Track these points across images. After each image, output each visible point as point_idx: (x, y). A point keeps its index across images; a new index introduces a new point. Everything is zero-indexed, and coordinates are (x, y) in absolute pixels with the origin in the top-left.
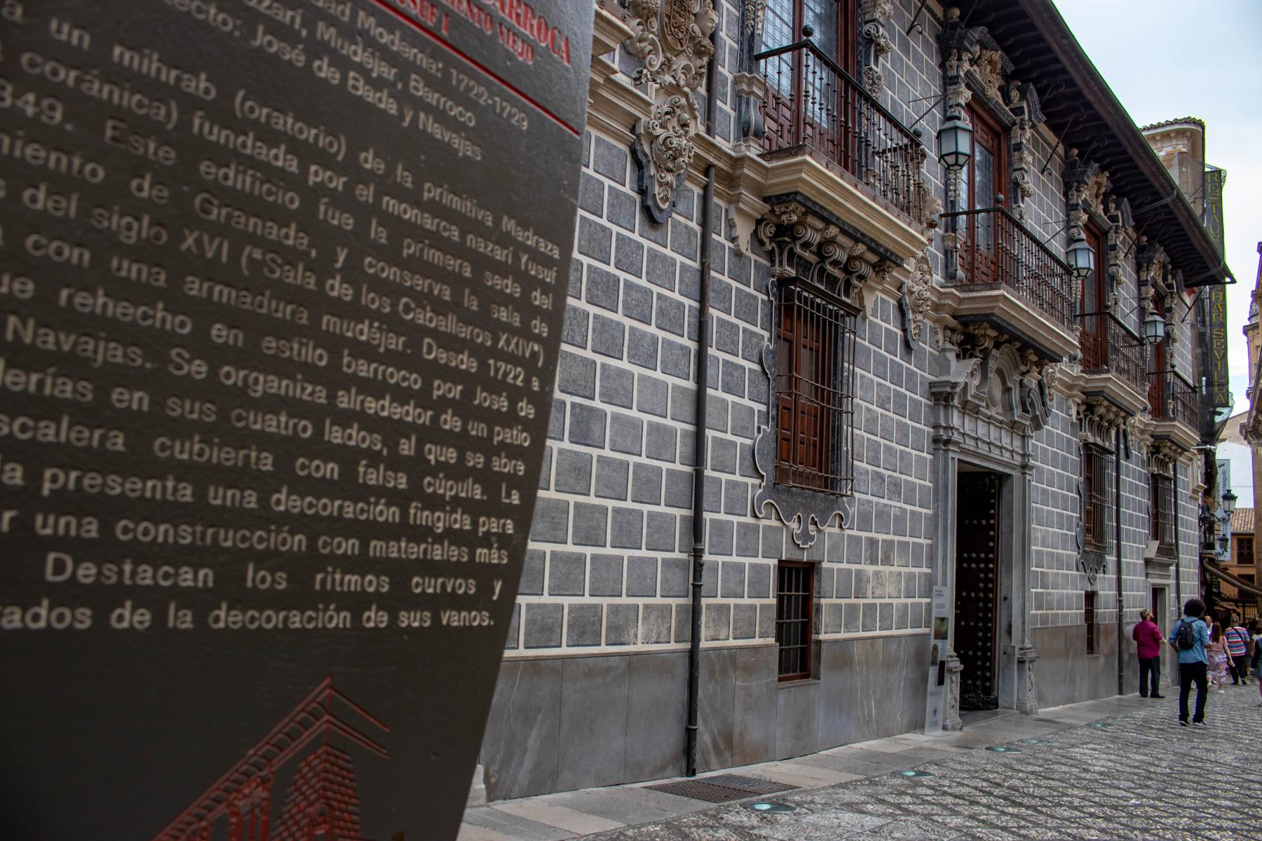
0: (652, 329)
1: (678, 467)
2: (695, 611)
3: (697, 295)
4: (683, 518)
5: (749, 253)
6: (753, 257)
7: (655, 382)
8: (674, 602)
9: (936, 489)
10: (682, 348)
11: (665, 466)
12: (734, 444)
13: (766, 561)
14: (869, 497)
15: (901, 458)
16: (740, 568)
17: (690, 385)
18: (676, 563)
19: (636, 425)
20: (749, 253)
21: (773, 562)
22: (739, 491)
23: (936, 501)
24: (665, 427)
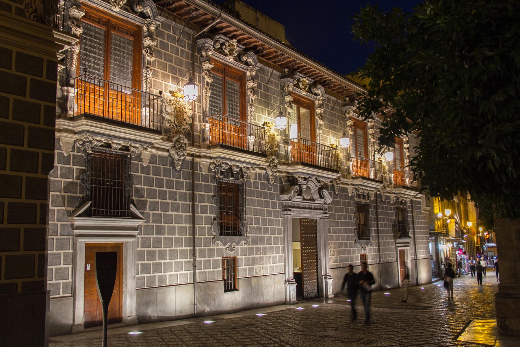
0: (178, 201)
1: (188, 236)
2: (194, 274)
3: (191, 189)
4: (190, 250)
5: (208, 173)
6: (209, 174)
7: (179, 216)
8: (188, 272)
9: (284, 229)
10: (187, 204)
11: (183, 237)
12: (205, 227)
13: (218, 258)
14: (256, 235)
15: (269, 221)
16: (209, 261)
17: (191, 214)
18: (189, 262)
19: (174, 228)
20: (208, 173)
21: (220, 258)
22: (208, 240)
23: (284, 232)
24: (183, 227)
